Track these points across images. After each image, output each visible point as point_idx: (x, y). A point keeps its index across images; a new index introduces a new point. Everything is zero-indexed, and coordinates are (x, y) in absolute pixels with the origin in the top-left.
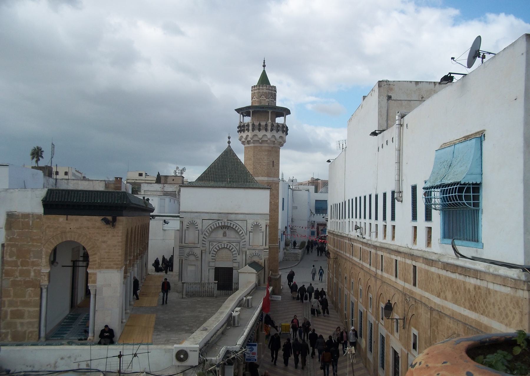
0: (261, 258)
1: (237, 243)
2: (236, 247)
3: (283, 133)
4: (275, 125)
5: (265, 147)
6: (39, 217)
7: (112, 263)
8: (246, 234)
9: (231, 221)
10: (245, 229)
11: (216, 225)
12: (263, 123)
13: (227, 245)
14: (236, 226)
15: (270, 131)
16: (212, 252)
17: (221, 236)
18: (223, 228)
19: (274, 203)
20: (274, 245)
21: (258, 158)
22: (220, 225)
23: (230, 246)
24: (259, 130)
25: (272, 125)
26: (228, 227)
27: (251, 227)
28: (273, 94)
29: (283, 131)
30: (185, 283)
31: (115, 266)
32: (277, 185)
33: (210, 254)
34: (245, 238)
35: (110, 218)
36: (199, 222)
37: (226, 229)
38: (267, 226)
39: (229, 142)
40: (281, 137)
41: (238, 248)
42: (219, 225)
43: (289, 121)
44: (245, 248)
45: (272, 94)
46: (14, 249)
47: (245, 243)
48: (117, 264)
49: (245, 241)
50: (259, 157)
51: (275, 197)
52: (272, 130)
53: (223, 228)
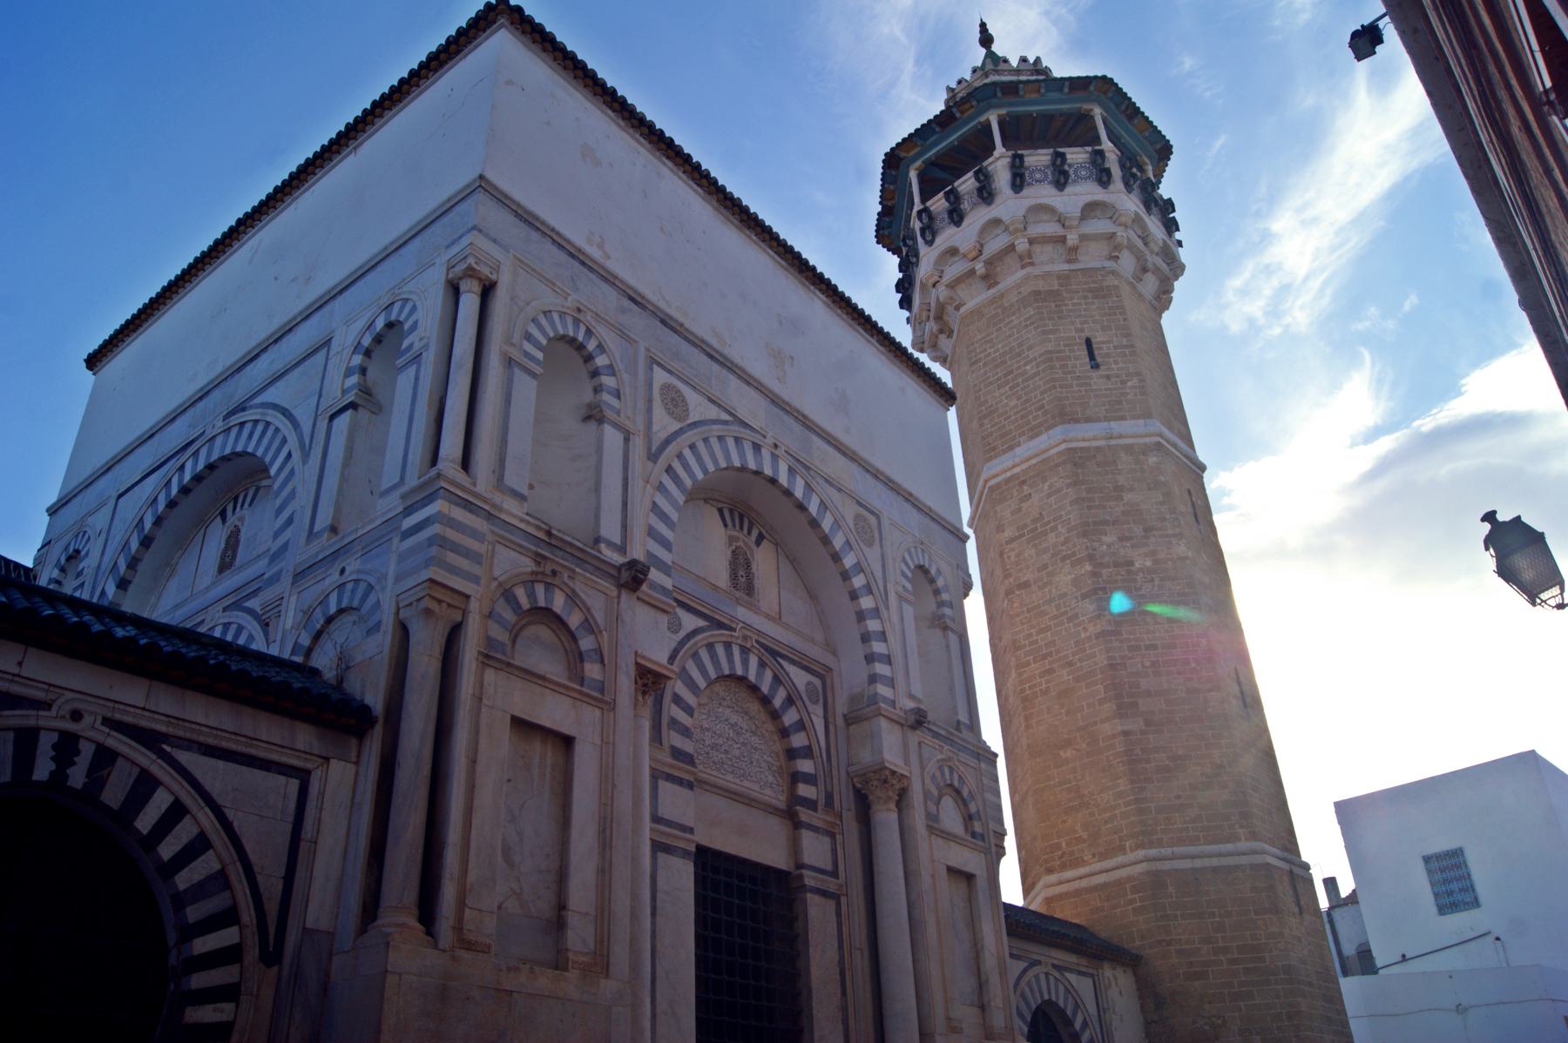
8: (306, 455)
9: (241, 408)
19: (1156, 562)
32: (1152, 460)
50: (997, 350)
51: (1147, 530)
52: (1019, 181)
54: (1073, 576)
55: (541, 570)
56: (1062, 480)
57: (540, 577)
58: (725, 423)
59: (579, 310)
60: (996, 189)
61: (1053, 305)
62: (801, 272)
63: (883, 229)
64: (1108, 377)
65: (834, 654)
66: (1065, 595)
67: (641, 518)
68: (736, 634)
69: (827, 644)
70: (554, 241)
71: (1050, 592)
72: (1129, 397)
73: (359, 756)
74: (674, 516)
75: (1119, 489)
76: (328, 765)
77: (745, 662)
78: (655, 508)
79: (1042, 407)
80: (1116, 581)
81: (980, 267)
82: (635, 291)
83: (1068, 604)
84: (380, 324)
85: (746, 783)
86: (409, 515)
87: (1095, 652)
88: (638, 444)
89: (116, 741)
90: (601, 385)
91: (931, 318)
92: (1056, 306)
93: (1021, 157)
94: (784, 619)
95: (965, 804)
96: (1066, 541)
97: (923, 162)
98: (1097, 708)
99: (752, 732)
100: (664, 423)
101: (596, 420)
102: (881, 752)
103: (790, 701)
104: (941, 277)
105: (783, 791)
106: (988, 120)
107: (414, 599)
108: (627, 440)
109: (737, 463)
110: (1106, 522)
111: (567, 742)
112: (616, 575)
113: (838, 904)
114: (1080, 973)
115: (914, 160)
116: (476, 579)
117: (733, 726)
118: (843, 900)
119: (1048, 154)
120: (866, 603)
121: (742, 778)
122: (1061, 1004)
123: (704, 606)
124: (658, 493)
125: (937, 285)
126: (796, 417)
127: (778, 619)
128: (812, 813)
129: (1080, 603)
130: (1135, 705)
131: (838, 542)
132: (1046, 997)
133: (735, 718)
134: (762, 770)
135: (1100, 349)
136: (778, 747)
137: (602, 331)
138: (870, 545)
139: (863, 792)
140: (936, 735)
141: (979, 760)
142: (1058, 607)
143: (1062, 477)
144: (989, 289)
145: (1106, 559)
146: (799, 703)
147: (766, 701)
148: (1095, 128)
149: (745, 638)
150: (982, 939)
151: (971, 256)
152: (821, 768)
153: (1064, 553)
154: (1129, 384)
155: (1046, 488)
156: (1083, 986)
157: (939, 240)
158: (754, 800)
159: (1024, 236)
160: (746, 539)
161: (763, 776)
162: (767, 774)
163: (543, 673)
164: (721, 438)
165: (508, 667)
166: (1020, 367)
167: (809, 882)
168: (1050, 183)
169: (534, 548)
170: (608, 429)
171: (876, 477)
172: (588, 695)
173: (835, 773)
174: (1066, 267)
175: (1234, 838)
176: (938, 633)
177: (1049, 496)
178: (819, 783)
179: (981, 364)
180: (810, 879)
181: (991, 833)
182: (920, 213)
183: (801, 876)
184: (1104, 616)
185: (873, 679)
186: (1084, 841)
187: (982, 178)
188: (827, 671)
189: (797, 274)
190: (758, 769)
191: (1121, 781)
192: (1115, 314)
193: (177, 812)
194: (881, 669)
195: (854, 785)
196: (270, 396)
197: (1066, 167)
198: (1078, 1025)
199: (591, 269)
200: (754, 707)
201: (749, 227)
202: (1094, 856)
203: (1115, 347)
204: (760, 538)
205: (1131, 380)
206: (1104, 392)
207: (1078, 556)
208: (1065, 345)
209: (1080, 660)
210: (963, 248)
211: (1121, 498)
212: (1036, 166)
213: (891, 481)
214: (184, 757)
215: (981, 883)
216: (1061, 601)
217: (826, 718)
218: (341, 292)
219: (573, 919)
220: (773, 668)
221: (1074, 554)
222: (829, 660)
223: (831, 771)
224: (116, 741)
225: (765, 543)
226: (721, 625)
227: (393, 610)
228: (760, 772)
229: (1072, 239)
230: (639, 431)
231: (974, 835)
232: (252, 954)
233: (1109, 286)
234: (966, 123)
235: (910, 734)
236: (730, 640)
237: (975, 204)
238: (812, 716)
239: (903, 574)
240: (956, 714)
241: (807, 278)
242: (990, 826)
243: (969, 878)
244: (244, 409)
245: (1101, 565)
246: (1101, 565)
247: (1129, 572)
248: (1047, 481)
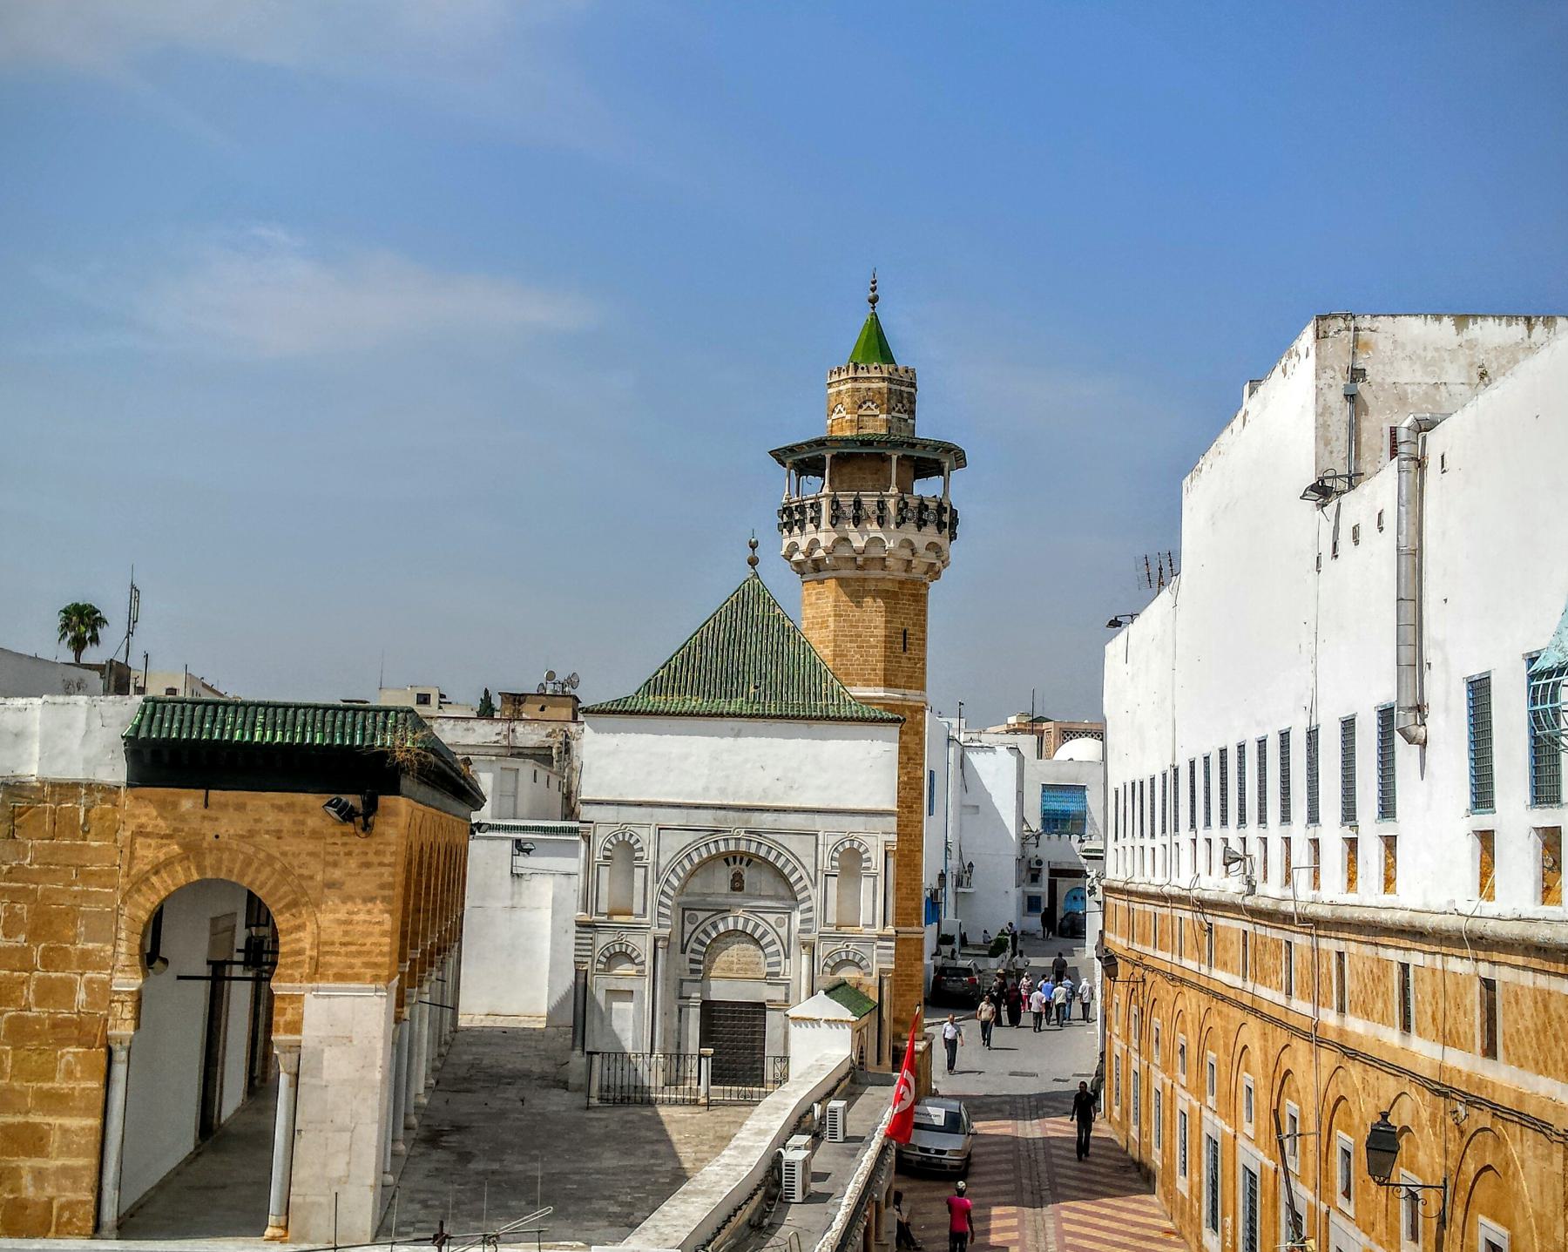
0: (868, 970)
1: (782, 916)
2: (778, 929)
3: (940, 532)
4: (913, 503)
5: (877, 580)
6: (110, 791)
7: (357, 961)
10: (808, 862)
11: (709, 851)
12: (869, 501)
13: (747, 921)
14: (779, 855)
16: (693, 945)
17: (726, 888)
18: (731, 860)
20: (910, 929)
21: (851, 621)
22: (722, 849)
23: (757, 926)
25: (903, 507)
26: (750, 860)
28: (905, 395)
29: (940, 526)
30: (598, 1053)
31: (369, 972)
32: (919, 717)
33: (683, 951)
34: (809, 898)
35: (353, 800)
36: (646, 835)
37: (741, 863)
38: (889, 855)
39: (753, 562)
40: (932, 547)
41: (783, 931)
42: (717, 849)
43: (959, 489)
44: (809, 931)
45: (902, 397)
46: (22, 908)
47: (809, 915)
48: (376, 965)
49: (810, 910)
51: (909, 759)
53: (731, 860)
81: (860, 560)
166: (866, 636)
174: (903, 576)
175: (911, 925)
210: (855, 545)
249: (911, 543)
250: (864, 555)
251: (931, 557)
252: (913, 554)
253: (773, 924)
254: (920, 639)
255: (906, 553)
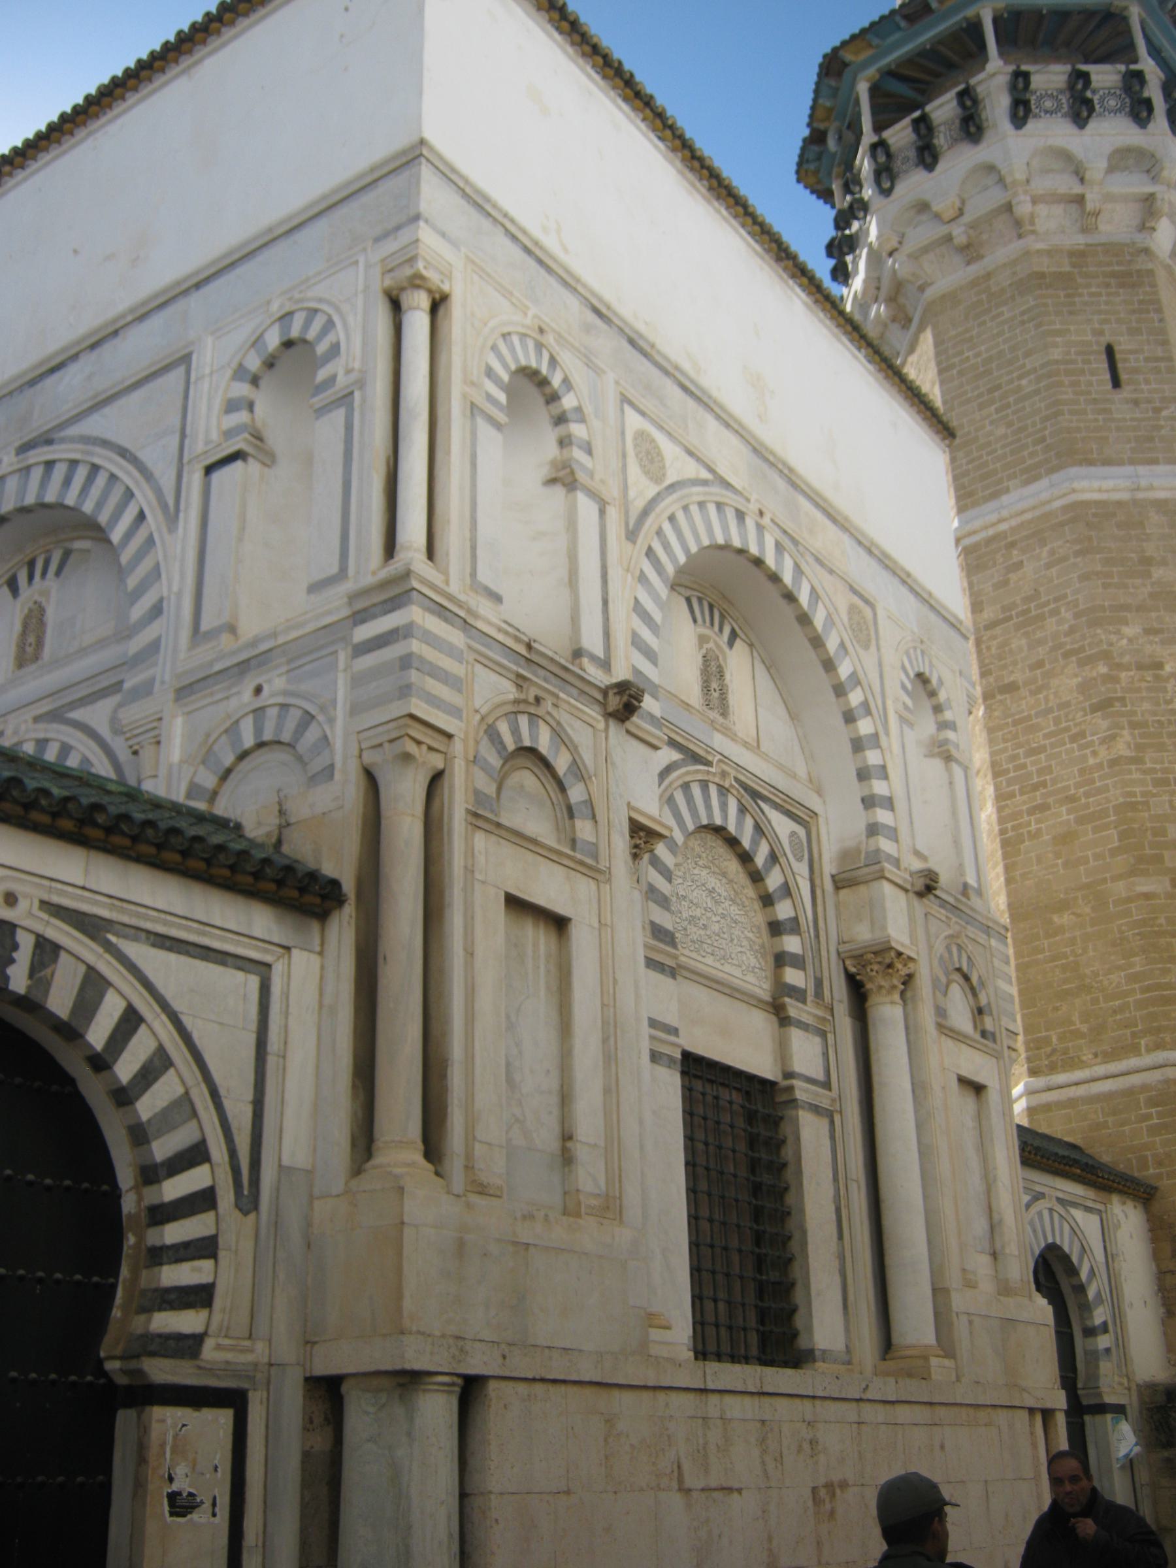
8: (172, 518)
9: (47, 440)
15: (1006, 125)
24: (929, 160)
27: (231, 406)
40: (1122, 159)
50: (978, 355)
52: (1021, 111)
54: (1080, 679)
55: (523, 696)
56: (1068, 545)
57: (522, 707)
58: (705, 483)
59: (541, 331)
60: (987, 120)
61: (1062, 294)
62: (778, 259)
63: (808, 161)
64: (1136, 403)
65: (819, 793)
66: (1067, 704)
67: (624, 621)
68: (713, 770)
69: (811, 781)
70: (507, 231)
71: (1046, 699)
72: (1163, 432)
73: (322, 944)
74: (657, 616)
75: (1147, 561)
76: (290, 957)
77: (724, 807)
78: (638, 607)
79: (1043, 439)
80: (1139, 690)
82: (601, 300)
83: (1070, 717)
84: (273, 340)
85: (727, 968)
86: (363, 621)
87: (1107, 785)
88: (613, 513)
89: (58, 932)
90: (569, 436)
91: (881, 298)
92: (1067, 296)
93: (1026, 76)
94: (763, 749)
95: (975, 994)
96: (1072, 631)
97: (879, 70)
98: (1108, 860)
99: (731, 900)
100: (642, 489)
101: (564, 485)
102: (884, 928)
103: (773, 858)
104: (900, 243)
105: (766, 977)
106: (978, 16)
107: (386, 738)
108: (602, 512)
109: (721, 541)
110: (1125, 608)
111: (559, 923)
112: (602, 700)
113: (832, 1123)
114: (1088, 1209)
115: (865, 65)
116: (455, 712)
117: (711, 891)
118: (837, 1118)
119: (1064, 73)
120: (865, 727)
121: (723, 961)
122: (1066, 1248)
123: (677, 733)
124: (639, 586)
125: (896, 255)
126: (781, 471)
127: (755, 747)
128: (800, 1005)
129: (1089, 717)
130: (1159, 859)
131: (832, 645)
132: (1050, 1240)
133: (713, 882)
134: (743, 950)
135: (1125, 360)
136: (759, 918)
137: (566, 358)
138: (866, 647)
139: (858, 977)
140: (944, 903)
141: (989, 935)
142: (1057, 721)
143: (1068, 541)
144: (968, 263)
145: (1126, 659)
146: (782, 860)
147: (745, 858)
148: (1128, 32)
149: (724, 774)
150: (995, 1168)
151: (947, 216)
152: (809, 946)
153: (1068, 647)
154: (1165, 413)
155: (1045, 554)
156: (1089, 1224)
157: (901, 189)
158: (737, 990)
159: (1026, 192)
160: (717, 639)
161: (744, 958)
162: (748, 953)
163: (534, 836)
164: (702, 505)
165: (498, 828)
166: (1011, 381)
167: (799, 1095)
168: (1065, 116)
169: (514, 668)
170: (581, 498)
171: (870, 552)
172: (582, 863)
173: (824, 953)
174: (1080, 240)
176: (937, 764)
177: (1048, 566)
178: (807, 967)
179: (955, 372)
180: (803, 1091)
181: (1003, 1031)
182: (874, 147)
183: (790, 1089)
184: (1122, 736)
185: (873, 830)
186: (1082, 1036)
187: (969, 103)
188: (811, 817)
189: (773, 263)
190: (740, 949)
191: (1137, 959)
192: (1148, 312)
193: (131, 1020)
194: (883, 816)
195: (846, 970)
196: (93, 426)
197: (1089, 94)
198: (1084, 1275)
199: (549, 270)
200: (733, 866)
201: (718, 198)
202: (1096, 1055)
203: (1147, 360)
204: (734, 635)
205: (1166, 408)
206: (1129, 423)
207: (1088, 653)
208: (1078, 353)
209: (1087, 795)
211: (1149, 575)
212: (1046, 91)
213: (887, 556)
214: (137, 951)
215: (993, 1096)
216: (1062, 713)
217: (812, 881)
218: (198, 286)
219: (581, 1153)
220: (754, 814)
221: (1082, 649)
222: (814, 803)
223: (820, 950)
224: (58, 932)
225: (738, 643)
226: (696, 758)
227: (356, 753)
228: (741, 952)
229: (1093, 200)
230: (614, 499)
231: (984, 1034)
232: (226, 1198)
233: (1138, 271)
234: (945, 16)
235: (916, 902)
236: (706, 778)
237: (956, 140)
238: (797, 877)
239: (903, 687)
240: (962, 874)
241: (785, 269)
242: (1003, 1023)
243: (978, 1089)
244: (49, 442)
245: (1120, 667)
246: (1120, 667)
247: (1157, 678)
248: (1046, 545)
249: (1065, 156)
250: (967, 218)
251: (1134, 184)
252: (1082, 180)
253: (105, 731)
254: (1157, 359)
255: (1066, 184)
